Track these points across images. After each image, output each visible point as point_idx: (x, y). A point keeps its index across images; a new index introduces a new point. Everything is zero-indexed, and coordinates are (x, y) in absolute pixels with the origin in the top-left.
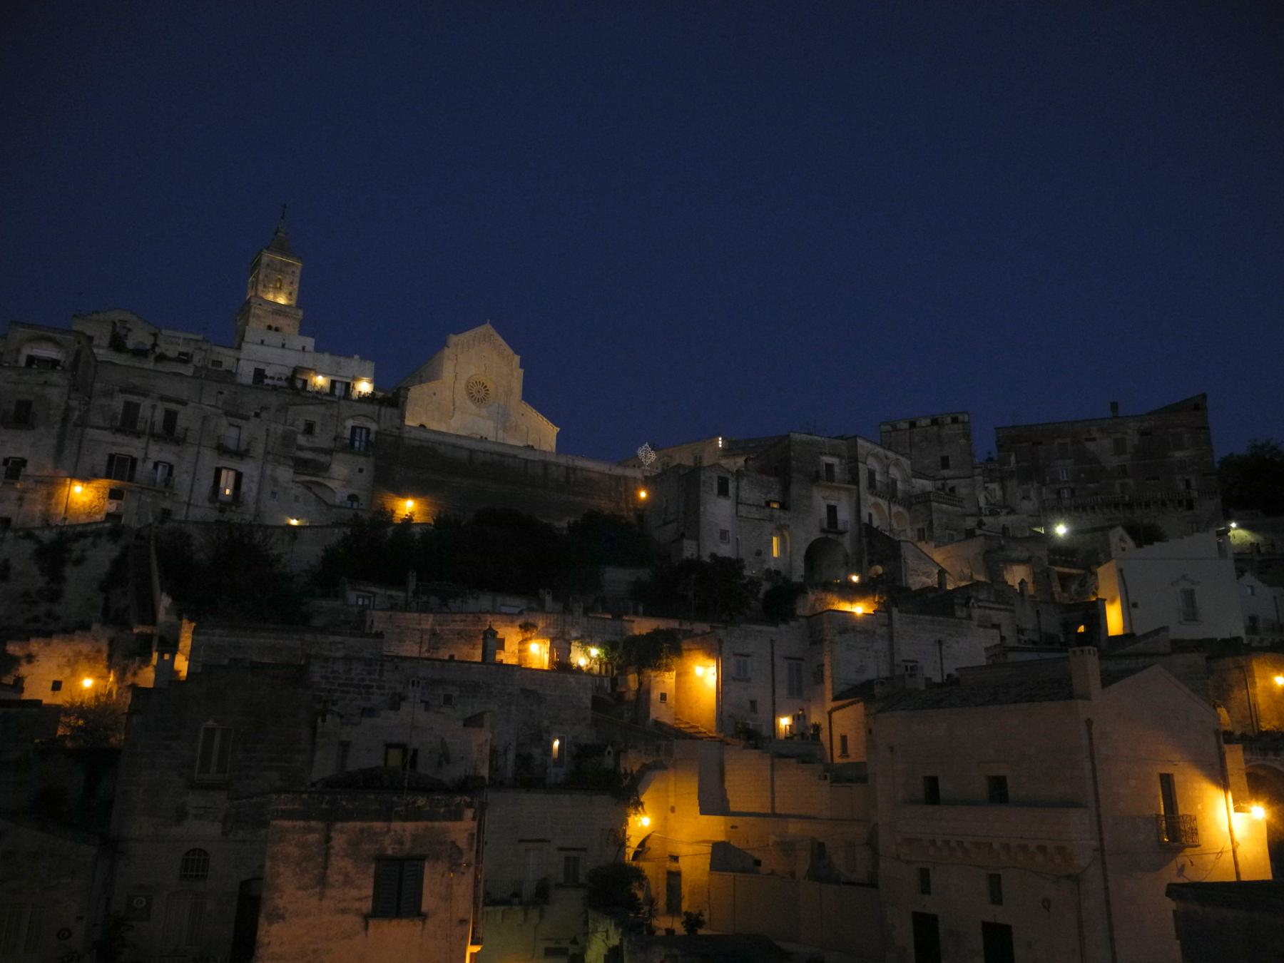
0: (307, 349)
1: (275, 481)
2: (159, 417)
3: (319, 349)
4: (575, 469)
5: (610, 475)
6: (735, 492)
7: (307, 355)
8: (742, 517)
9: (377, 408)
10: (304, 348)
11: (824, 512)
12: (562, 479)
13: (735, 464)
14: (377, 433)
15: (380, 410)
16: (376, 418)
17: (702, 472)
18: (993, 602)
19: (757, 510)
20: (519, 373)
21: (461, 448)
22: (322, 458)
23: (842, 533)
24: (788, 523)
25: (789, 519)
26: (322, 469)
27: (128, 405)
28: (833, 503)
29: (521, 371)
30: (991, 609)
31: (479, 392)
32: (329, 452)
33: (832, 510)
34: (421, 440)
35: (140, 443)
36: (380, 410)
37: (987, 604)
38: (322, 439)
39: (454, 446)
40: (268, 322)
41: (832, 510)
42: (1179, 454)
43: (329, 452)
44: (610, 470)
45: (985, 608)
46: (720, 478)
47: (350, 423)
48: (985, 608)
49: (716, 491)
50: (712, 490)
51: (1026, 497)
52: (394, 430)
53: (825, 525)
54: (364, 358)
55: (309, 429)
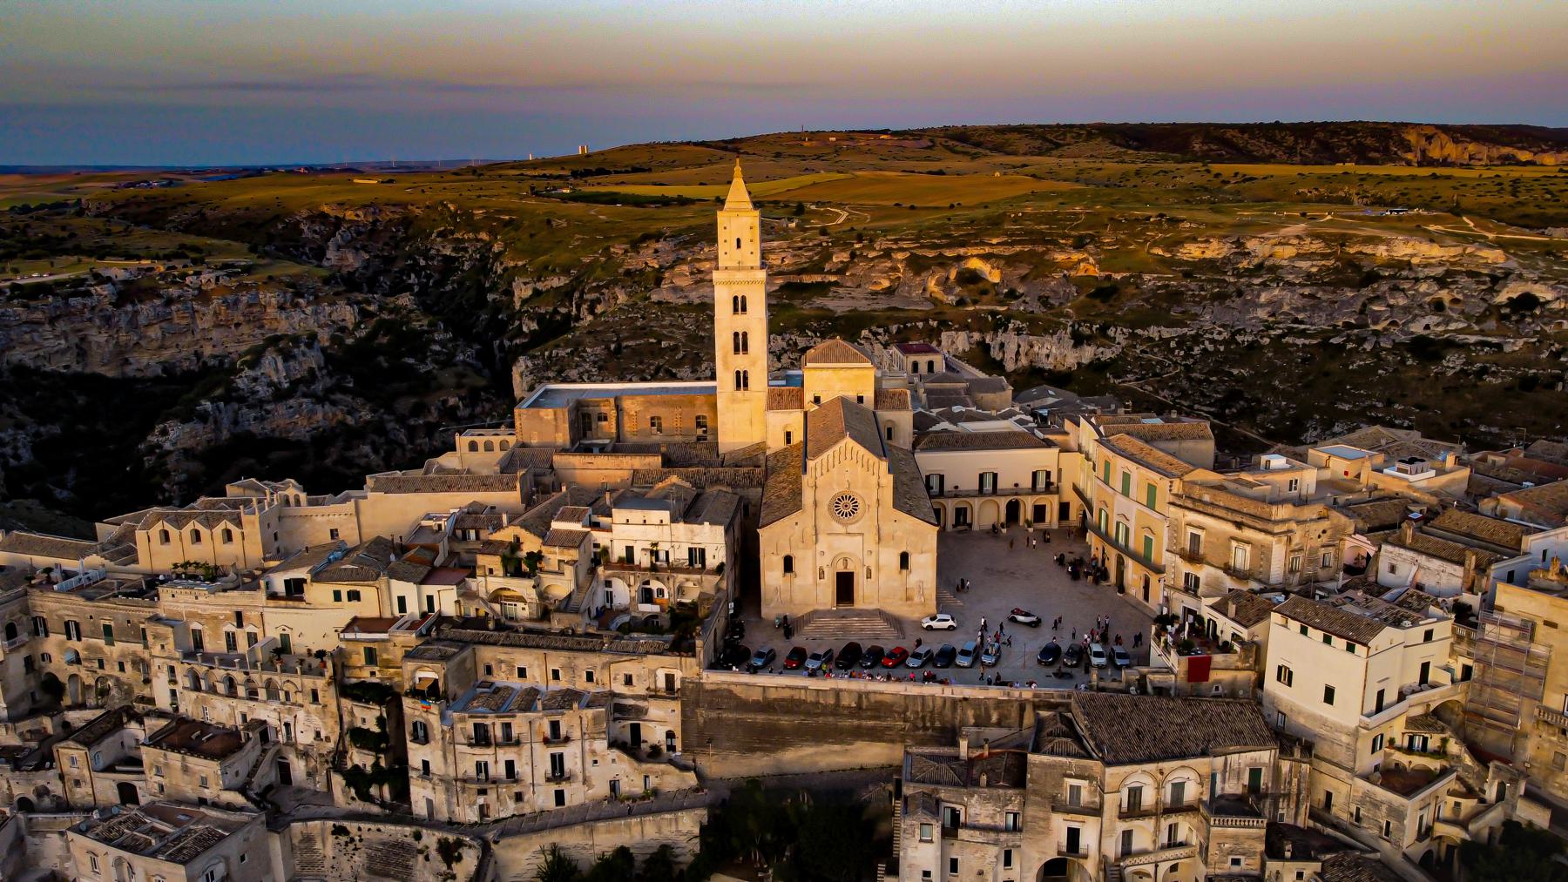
1: (593, 752)
2: (499, 732)
3: (674, 520)
4: (868, 693)
11: (1063, 839)
12: (854, 705)
20: (888, 480)
21: (754, 686)
22: (641, 703)
23: (1085, 857)
26: (640, 712)
27: (476, 726)
28: (1075, 825)
29: (891, 477)
32: (644, 698)
33: (1073, 835)
35: (490, 751)
38: (639, 688)
39: (747, 684)
41: (1073, 835)
43: (644, 698)
53: (1064, 849)
54: (712, 523)
55: (628, 681)
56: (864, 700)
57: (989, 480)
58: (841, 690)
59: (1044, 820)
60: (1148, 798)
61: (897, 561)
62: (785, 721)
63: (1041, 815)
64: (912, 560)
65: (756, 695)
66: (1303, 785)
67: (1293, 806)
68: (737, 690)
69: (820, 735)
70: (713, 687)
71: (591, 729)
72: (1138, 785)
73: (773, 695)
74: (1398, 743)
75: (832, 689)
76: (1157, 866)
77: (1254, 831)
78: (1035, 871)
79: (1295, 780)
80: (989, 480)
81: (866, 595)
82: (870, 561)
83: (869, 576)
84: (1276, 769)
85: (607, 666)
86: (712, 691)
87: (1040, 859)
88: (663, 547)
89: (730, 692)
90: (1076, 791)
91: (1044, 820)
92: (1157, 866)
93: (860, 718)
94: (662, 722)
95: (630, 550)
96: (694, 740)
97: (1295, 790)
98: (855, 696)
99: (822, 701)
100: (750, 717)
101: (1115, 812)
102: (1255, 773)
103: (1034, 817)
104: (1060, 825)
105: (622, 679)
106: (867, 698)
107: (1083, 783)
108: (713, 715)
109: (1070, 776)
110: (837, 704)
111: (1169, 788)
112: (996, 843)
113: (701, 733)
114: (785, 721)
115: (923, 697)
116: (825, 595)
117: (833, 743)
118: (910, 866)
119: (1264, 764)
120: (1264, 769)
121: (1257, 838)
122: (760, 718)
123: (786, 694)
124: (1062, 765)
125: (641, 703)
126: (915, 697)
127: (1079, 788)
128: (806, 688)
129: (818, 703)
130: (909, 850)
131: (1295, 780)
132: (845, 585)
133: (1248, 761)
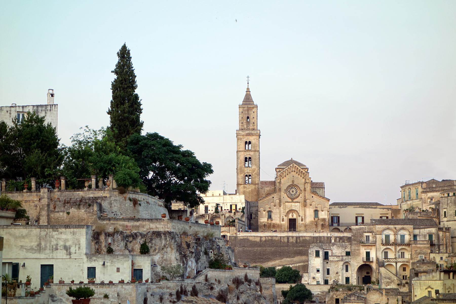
0: (221, 195)
4: (299, 237)
5: (313, 237)
6: (322, 255)
7: (221, 197)
8: (331, 261)
9: (228, 228)
10: (220, 194)
13: (427, 195)
14: (230, 237)
15: (229, 228)
16: (228, 232)
17: (309, 250)
18: (356, 300)
19: (337, 258)
21: (257, 237)
23: (372, 262)
24: (350, 260)
25: (350, 259)
28: (368, 251)
30: (355, 302)
31: (293, 191)
33: (368, 254)
34: (243, 237)
36: (229, 228)
37: (353, 301)
40: (245, 140)
44: (314, 235)
45: (353, 302)
46: (316, 251)
48: (353, 302)
49: (315, 255)
50: (313, 256)
52: (235, 234)
53: (365, 260)
56: (298, 240)
57: (360, 220)
58: (289, 237)
59: (358, 250)
60: (392, 238)
62: (268, 249)
63: (357, 248)
65: (258, 240)
66: (447, 241)
67: (445, 248)
68: (251, 238)
70: (242, 238)
72: (388, 234)
73: (264, 239)
75: (286, 236)
76: (396, 264)
77: (427, 245)
78: (356, 270)
79: (444, 239)
80: (360, 220)
82: (301, 213)
83: (302, 220)
86: (241, 239)
87: (357, 265)
89: (248, 240)
90: (368, 237)
91: (358, 250)
92: (396, 264)
93: (297, 247)
97: (445, 242)
98: (295, 238)
99: (282, 241)
101: (380, 242)
102: (431, 236)
103: (355, 249)
104: (363, 251)
106: (300, 239)
108: (241, 249)
109: (366, 232)
110: (288, 241)
111: (399, 236)
112: (342, 260)
114: (268, 249)
115: (320, 237)
117: (287, 257)
118: (312, 267)
119: (434, 234)
120: (434, 236)
121: (428, 247)
122: (259, 249)
124: (363, 228)
126: (317, 237)
127: (369, 236)
128: (277, 237)
129: (281, 241)
130: (312, 262)
131: (444, 239)
133: (428, 232)
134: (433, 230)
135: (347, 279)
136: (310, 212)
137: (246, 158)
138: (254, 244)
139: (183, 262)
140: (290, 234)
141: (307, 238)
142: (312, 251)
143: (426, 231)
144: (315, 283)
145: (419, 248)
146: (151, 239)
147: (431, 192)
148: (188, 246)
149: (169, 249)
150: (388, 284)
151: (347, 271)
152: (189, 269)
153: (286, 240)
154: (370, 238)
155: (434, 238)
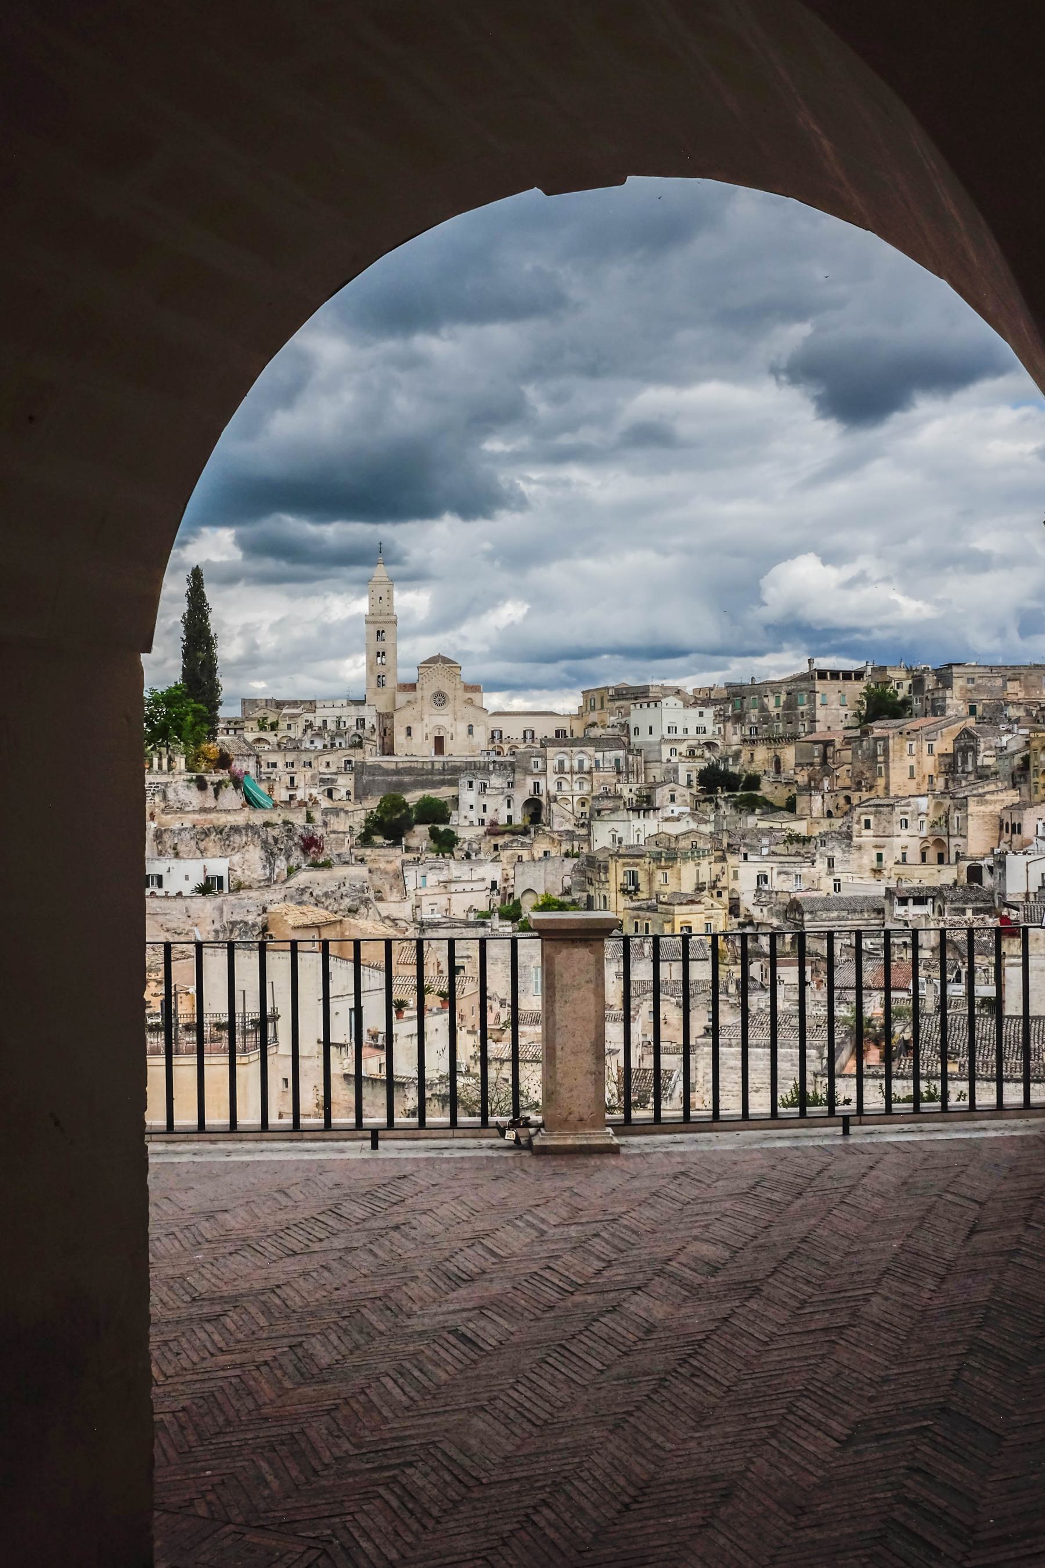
22: (334, 777)
26: (334, 781)
32: (336, 774)
42: (802, 708)
43: (336, 774)
47: (344, 759)
51: (735, 733)
57: (529, 735)
61: (466, 730)
62: (407, 779)
64: (475, 729)
65: (393, 766)
68: (383, 765)
69: (424, 785)
71: (310, 782)
73: (401, 766)
74: (684, 754)
81: (449, 746)
82: (451, 730)
84: (627, 759)
85: (317, 758)
88: (344, 719)
94: (345, 786)
95: (325, 722)
96: (360, 792)
100: (389, 778)
102: (617, 761)
104: (530, 782)
105: (325, 764)
107: (539, 760)
108: (371, 778)
112: (502, 794)
113: (364, 789)
114: (407, 779)
116: (430, 747)
122: (395, 778)
123: (408, 765)
125: (334, 777)
132: (439, 743)
134: (621, 753)
135: (510, 818)
136: (462, 728)
137: (378, 653)
138: (387, 772)
139: (270, 863)
140: (436, 758)
141: (458, 764)
142: (464, 781)
143: (611, 755)
144: (467, 824)
145: (603, 776)
146: (229, 836)
147: (619, 699)
148: (276, 840)
149: (252, 846)
150: (561, 824)
151: (509, 807)
152: (277, 870)
153: (430, 767)
154: (540, 764)
155: (622, 763)
